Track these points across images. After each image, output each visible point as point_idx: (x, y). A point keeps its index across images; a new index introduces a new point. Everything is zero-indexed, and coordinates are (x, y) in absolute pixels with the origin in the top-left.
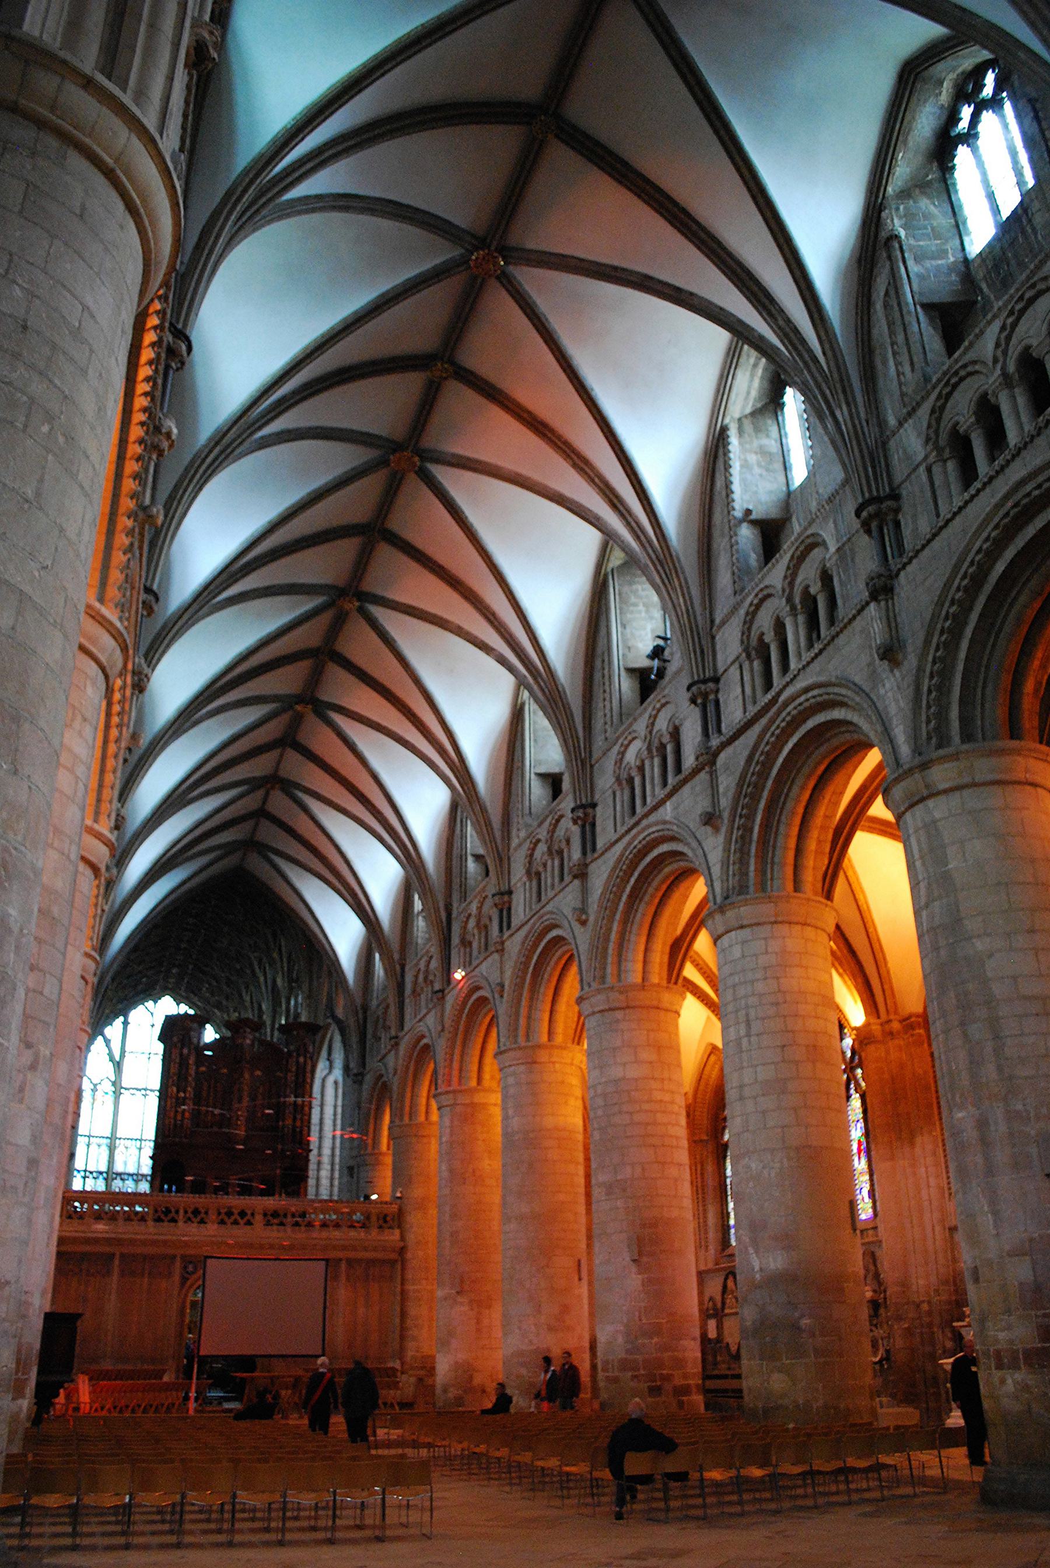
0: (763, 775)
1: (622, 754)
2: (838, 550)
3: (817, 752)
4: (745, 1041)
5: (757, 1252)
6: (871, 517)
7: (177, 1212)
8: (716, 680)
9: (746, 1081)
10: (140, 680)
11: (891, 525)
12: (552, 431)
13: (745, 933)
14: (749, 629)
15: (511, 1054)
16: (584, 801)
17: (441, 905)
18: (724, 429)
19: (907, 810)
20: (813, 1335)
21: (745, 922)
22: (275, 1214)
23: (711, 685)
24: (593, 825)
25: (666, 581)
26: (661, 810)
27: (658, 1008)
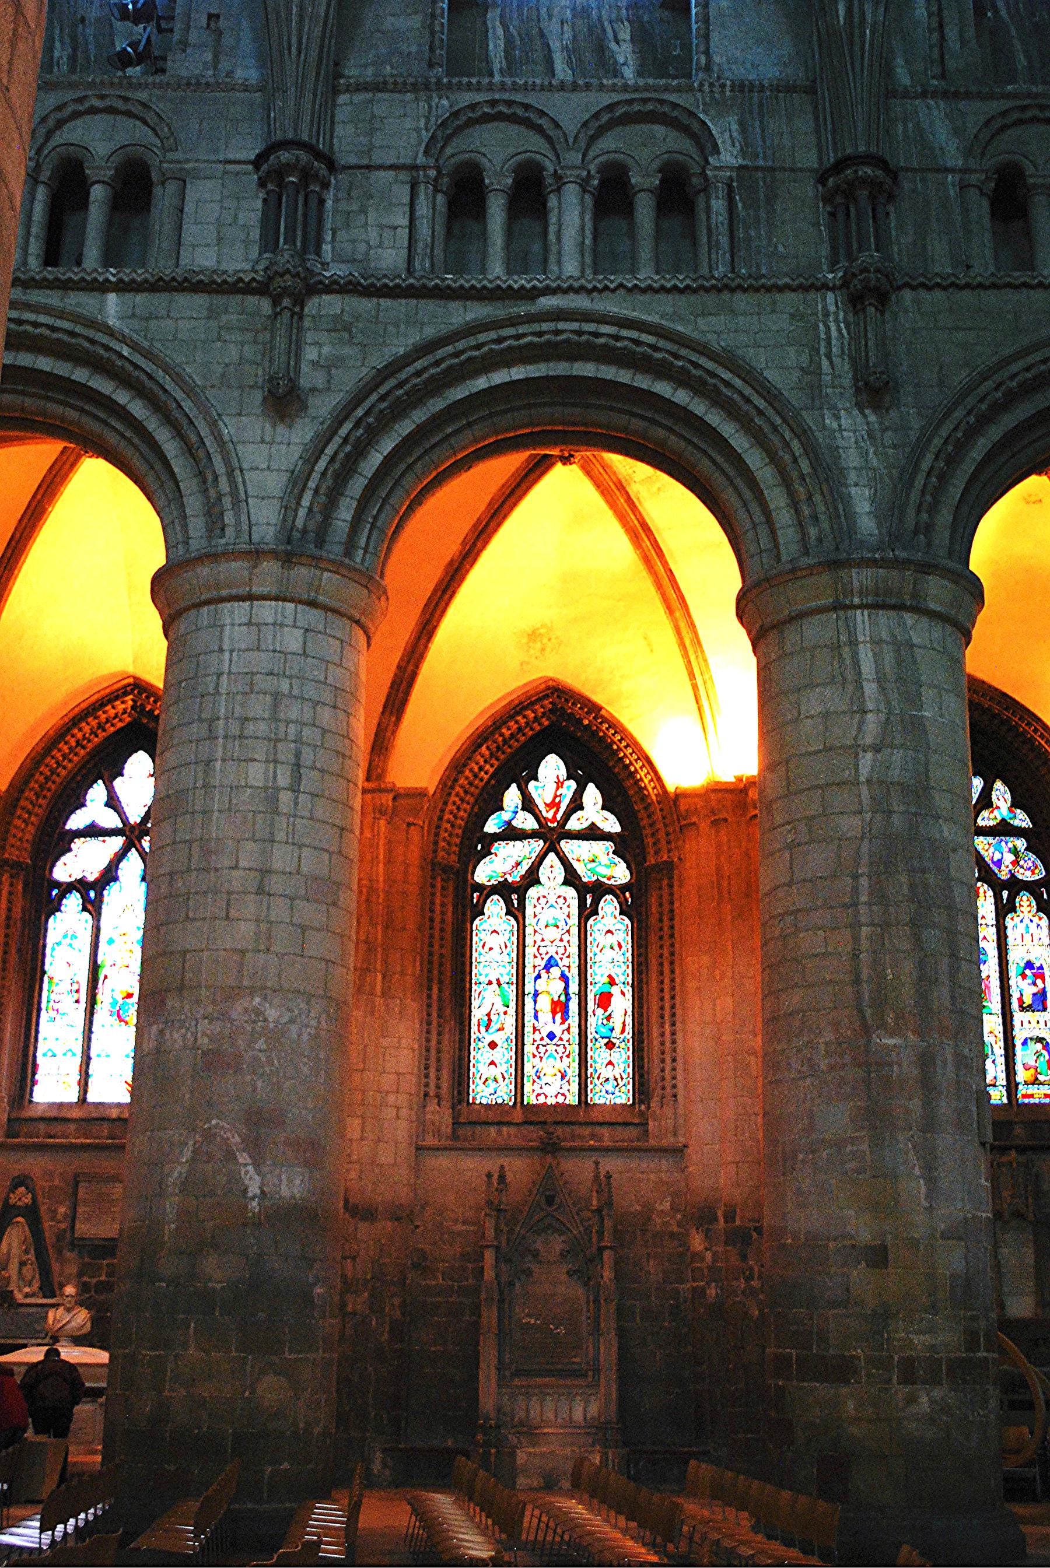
5: (257, 1165)
9: (277, 864)
13: (313, 616)
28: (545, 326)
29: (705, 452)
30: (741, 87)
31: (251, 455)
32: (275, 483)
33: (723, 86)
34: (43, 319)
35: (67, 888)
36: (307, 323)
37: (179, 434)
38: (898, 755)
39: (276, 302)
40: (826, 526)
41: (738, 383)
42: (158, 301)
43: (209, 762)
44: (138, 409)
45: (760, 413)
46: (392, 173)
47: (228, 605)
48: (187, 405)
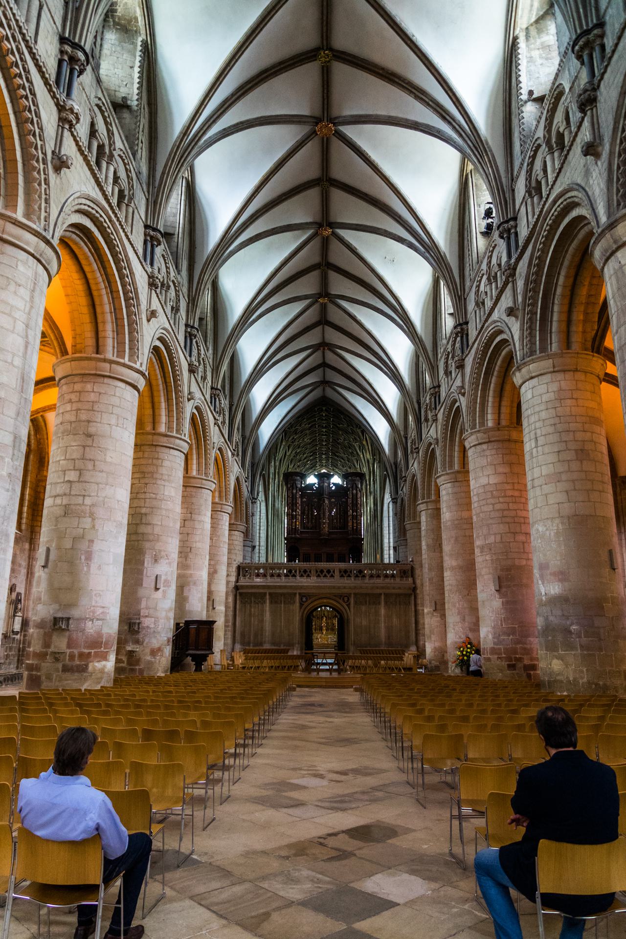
0: (538, 273)
1: (478, 286)
2: (571, 89)
4: (535, 450)
5: (543, 584)
6: (582, 49)
7: (296, 572)
8: (515, 219)
10: (154, 280)
11: (597, 49)
12: (399, 77)
13: (534, 382)
14: (530, 176)
15: (443, 478)
16: (461, 322)
17: (415, 400)
18: (515, 39)
19: (604, 265)
20: (580, 637)
21: (533, 374)
22: (346, 571)
23: (512, 223)
24: (467, 335)
25: (481, 160)
26: (493, 314)
27: (509, 440)
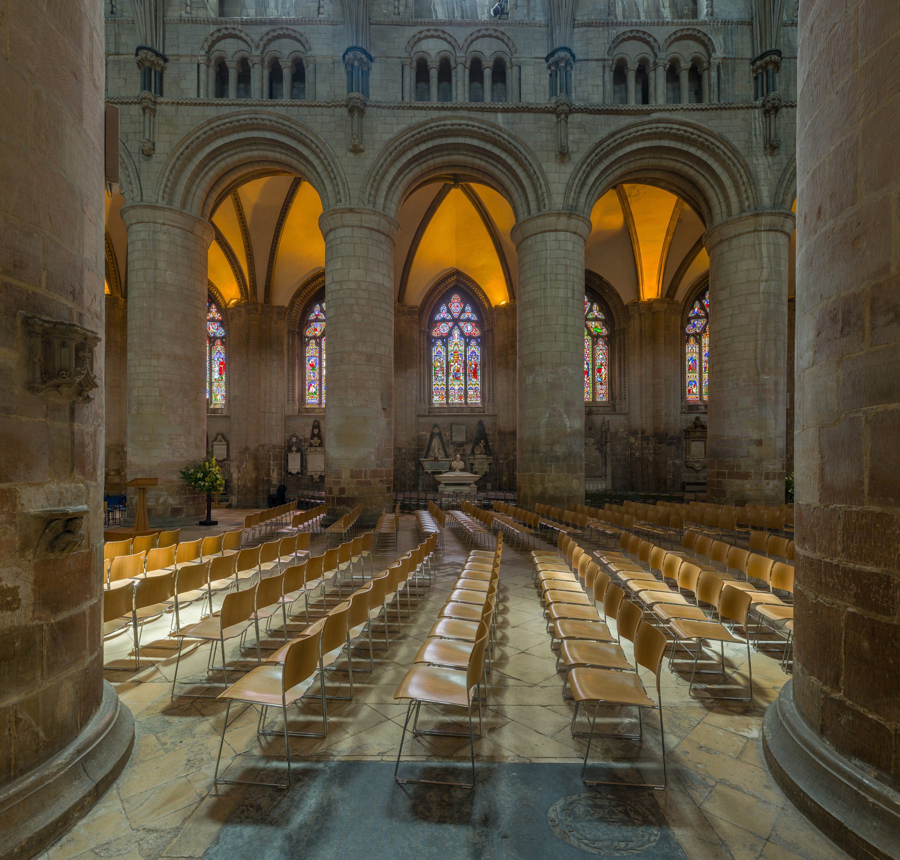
3: (647, 160)
21: (578, 231)
28: (654, 125)
29: (703, 176)
30: (725, 23)
31: (552, 177)
32: (561, 188)
33: (718, 22)
34: (476, 124)
35: (437, 339)
36: (569, 125)
37: (525, 170)
38: (773, 283)
39: (558, 117)
40: (751, 200)
41: (722, 147)
42: (516, 116)
43: (545, 289)
44: (510, 161)
45: (729, 158)
46: (595, 62)
47: (547, 233)
48: (529, 158)
